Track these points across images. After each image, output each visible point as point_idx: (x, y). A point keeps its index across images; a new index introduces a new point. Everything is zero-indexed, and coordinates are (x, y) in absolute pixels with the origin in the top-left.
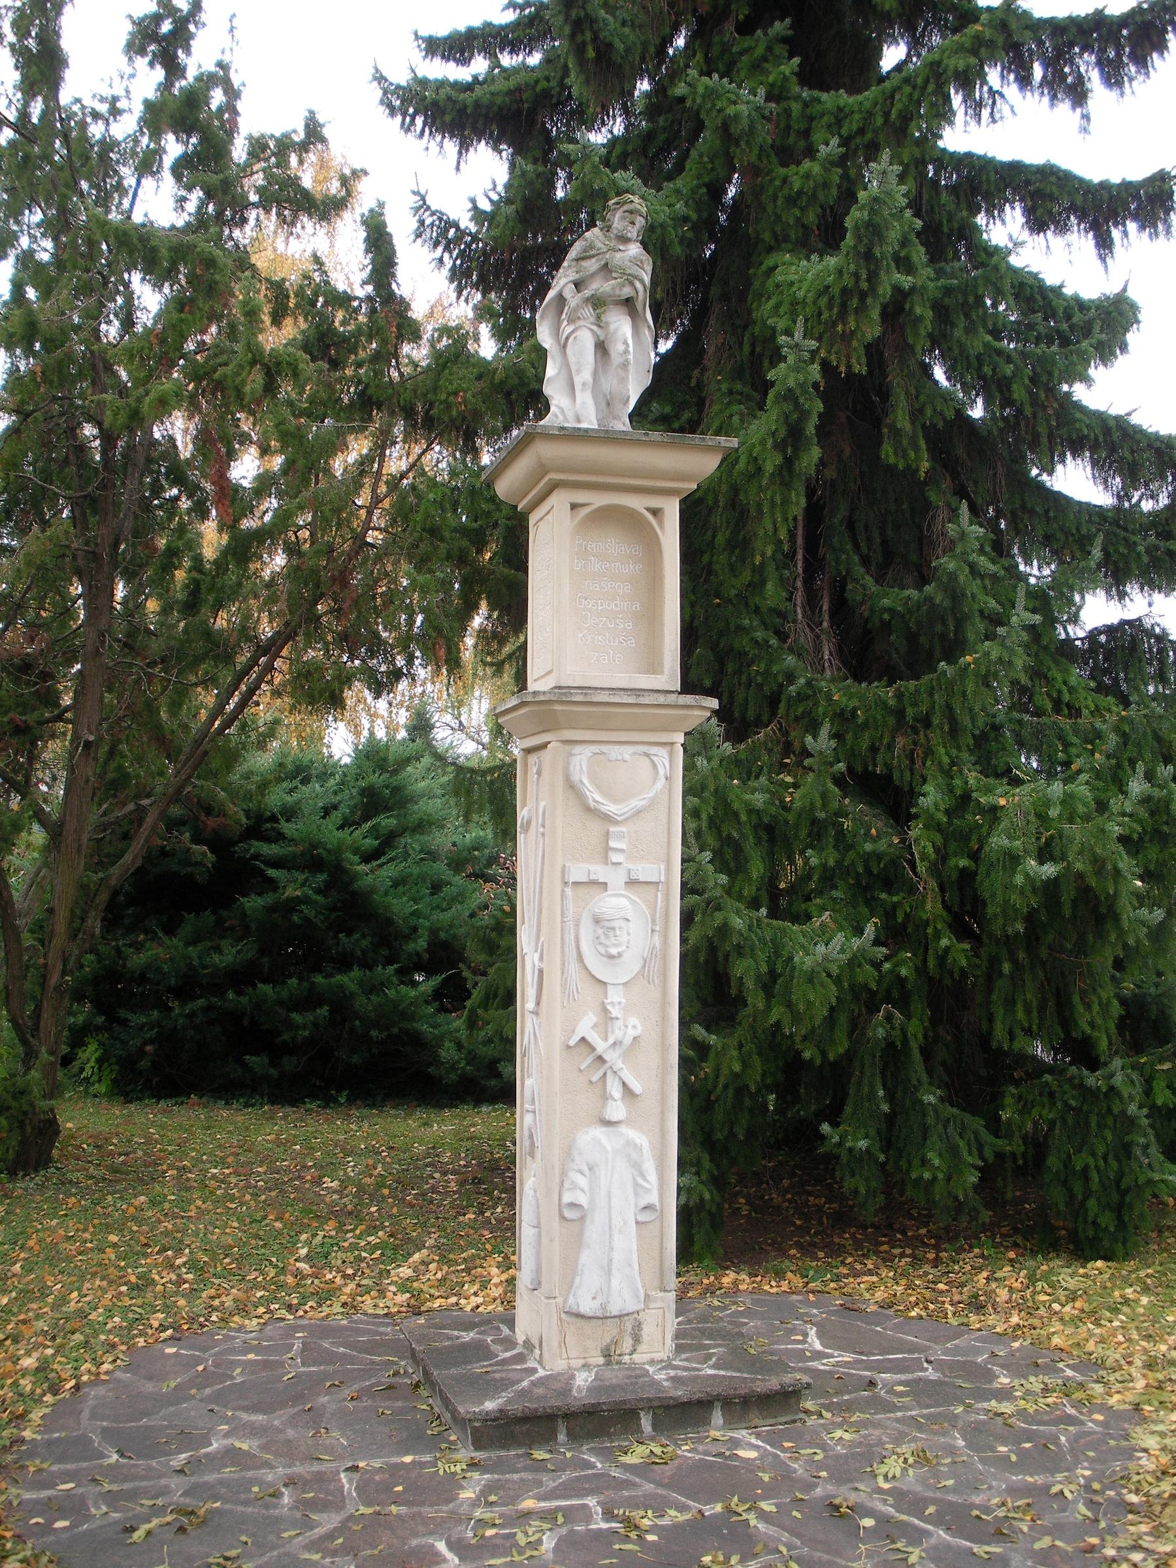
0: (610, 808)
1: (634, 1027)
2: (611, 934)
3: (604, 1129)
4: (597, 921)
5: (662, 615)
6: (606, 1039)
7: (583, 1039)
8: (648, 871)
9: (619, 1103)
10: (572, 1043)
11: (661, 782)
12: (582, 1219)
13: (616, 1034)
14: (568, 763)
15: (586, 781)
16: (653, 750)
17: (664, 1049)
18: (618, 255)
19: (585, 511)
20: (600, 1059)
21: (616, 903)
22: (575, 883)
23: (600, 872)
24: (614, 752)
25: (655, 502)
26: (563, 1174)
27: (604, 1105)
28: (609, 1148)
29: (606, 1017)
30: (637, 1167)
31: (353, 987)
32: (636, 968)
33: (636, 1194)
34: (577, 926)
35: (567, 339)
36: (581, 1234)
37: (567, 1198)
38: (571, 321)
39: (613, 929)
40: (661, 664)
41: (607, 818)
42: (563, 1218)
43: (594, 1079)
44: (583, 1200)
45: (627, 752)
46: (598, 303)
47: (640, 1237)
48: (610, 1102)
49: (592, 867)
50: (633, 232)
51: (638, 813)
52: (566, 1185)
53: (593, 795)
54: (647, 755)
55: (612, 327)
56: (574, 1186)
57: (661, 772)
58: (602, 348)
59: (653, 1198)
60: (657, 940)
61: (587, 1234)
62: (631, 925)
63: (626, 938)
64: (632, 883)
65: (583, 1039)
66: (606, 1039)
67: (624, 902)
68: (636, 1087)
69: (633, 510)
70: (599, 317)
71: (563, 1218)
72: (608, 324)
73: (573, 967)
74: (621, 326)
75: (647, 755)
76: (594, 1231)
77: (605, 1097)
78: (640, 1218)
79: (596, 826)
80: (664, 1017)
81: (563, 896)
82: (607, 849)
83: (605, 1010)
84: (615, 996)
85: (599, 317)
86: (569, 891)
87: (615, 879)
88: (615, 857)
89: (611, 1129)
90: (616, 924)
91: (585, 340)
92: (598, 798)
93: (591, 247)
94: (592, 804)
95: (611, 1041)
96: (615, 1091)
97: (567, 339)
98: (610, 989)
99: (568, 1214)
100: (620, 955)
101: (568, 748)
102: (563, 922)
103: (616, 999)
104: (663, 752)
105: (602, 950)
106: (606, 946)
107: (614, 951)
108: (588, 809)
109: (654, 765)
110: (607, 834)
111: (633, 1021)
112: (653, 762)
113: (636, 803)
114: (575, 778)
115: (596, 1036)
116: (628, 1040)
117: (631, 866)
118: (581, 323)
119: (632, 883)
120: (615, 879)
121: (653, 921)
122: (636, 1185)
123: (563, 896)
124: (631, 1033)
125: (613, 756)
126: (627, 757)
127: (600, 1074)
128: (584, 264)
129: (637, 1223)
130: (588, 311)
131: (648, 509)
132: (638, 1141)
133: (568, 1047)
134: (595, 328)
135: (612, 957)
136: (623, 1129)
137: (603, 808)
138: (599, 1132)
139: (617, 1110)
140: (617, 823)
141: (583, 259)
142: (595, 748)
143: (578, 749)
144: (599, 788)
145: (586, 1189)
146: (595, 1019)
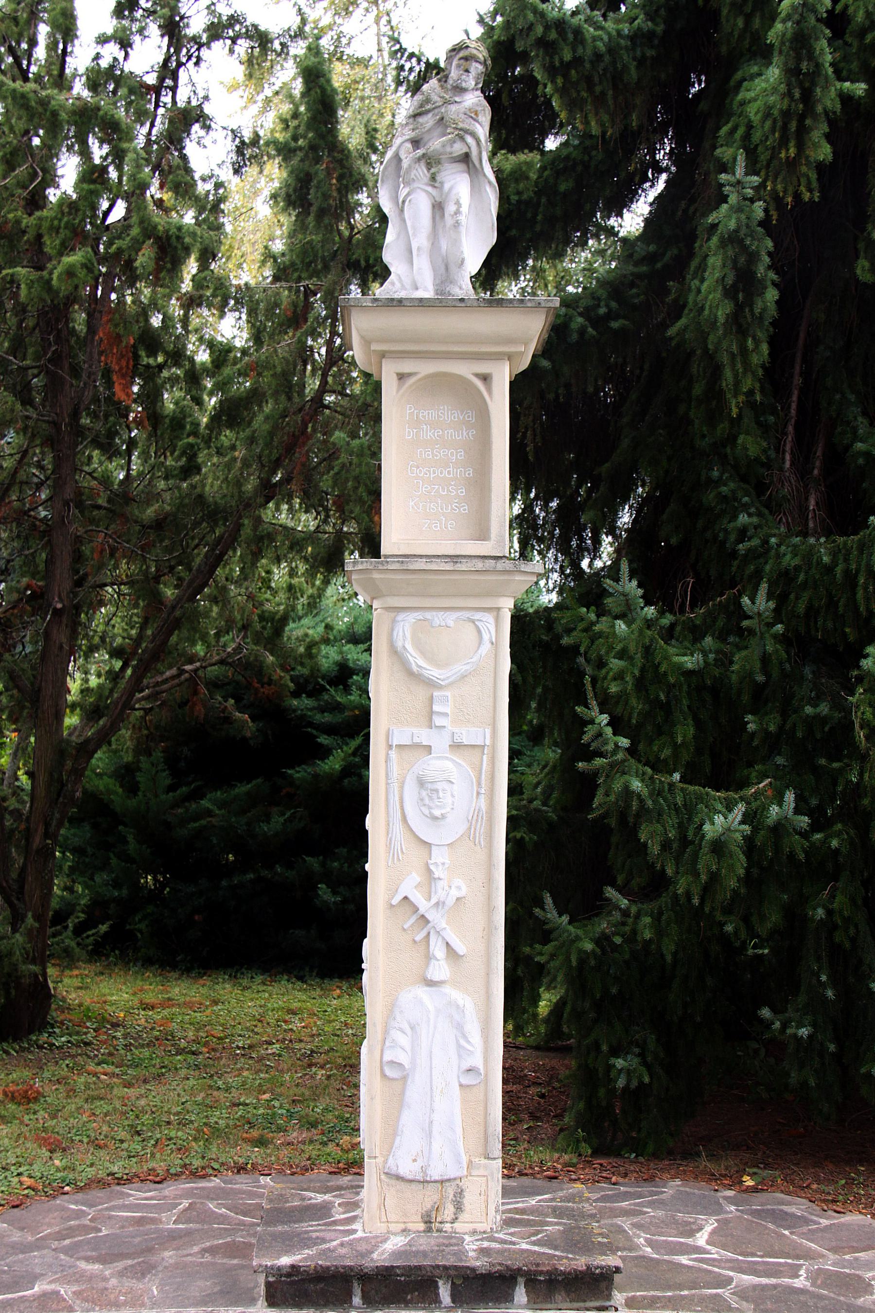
0: (433, 672)
1: (459, 888)
2: (435, 796)
3: (427, 988)
4: (421, 783)
5: (490, 482)
6: (429, 899)
7: (406, 898)
8: (469, 735)
9: (443, 963)
10: (394, 902)
11: (486, 647)
12: (404, 1078)
13: (440, 893)
14: (392, 630)
15: (409, 647)
16: (477, 616)
17: (490, 910)
18: (453, 108)
19: (412, 380)
20: (424, 920)
21: (443, 766)
22: (399, 746)
23: (424, 736)
24: (438, 618)
25: (483, 368)
26: (386, 1032)
27: (427, 965)
28: (431, 1008)
29: (430, 877)
30: (460, 1027)
31: (75, 92)
32: (462, 829)
33: (460, 1056)
34: (402, 787)
35: (404, 202)
36: (403, 1093)
37: (387, 1057)
38: (407, 183)
39: (437, 791)
40: (488, 529)
41: (431, 684)
42: (384, 1075)
43: (418, 938)
44: (403, 1058)
45: (451, 618)
46: (431, 161)
47: (464, 1101)
48: (433, 962)
49: (415, 730)
50: (470, 82)
51: (463, 677)
52: (387, 1044)
53: (416, 660)
54: (473, 622)
55: (447, 186)
56: (395, 1045)
57: (486, 637)
58: (438, 207)
59: (477, 1061)
60: (483, 803)
61: (408, 1093)
62: (455, 787)
63: (449, 800)
64: (456, 746)
65: (406, 898)
66: (429, 899)
67: (449, 765)
68: (461, 949)
69: (460, 377)
70: (433, 178)
71: (384, 1075)
72: (442, 183)
73: (398, 828)
74: (458, 185)
75: (473, 622)
76: (414, 1092)
77: (428, 957)
78: (464, 1082)
79: (421, 693)
80: (490, 879)
81: (387, 759)
82: (431, 713)
83: (430, 872)
84: (439, 857)
85: (433, 178)
86: (393, 754)
87: (440, 742)
88: (438, 721)
89: (433, 989)
90: (439, 786)
91: (420, 204)
92: (421, 662)
93: (428, 101)
94: (415, 668)
95: (434, 900)
96: (439, 951)
97: (404, 202)
98: (433, 848)
99: (388, 1072)
100: (443, 817)
101: (393, 615)
102: (387, 784)
103: (440, 860)
104: (488, 620)
105: (427, 812)
106: (430, 808)
107: (437, 813)
108: (410, 673)
109: (479, 632)
110: (431, 699)
111: (458, 882)
112: (477, 627)
113: (460, 668)
114: (399, 644)
115: (419, 896)
116: (450, 901)
117: (456, 730)
118: (415, 185)
119: (456, 746)
120: (440, 742)
121: (479, 784)
122: (459, 1046)
123: (387, 759)
124: (455, 893)
125: (437, 622)
126: (451, 623)
127: (423, 934)
128: (421, 120)
129: (461, 1085)
130: (421, 172)
131: (477, 375)
132: (461, 1002)
133: (392, 906)
134: (430, 189)
135: (435, 818)
136: (447, 989)
137: (426, 673)
138: (422, 992)
139: (440, 970)
140: (440, 687)
141: (419, 114)
142: (418, 615)
143: (401, 616)
144: (423, 653)
145: (408, 1048)
146: (418, 879)
